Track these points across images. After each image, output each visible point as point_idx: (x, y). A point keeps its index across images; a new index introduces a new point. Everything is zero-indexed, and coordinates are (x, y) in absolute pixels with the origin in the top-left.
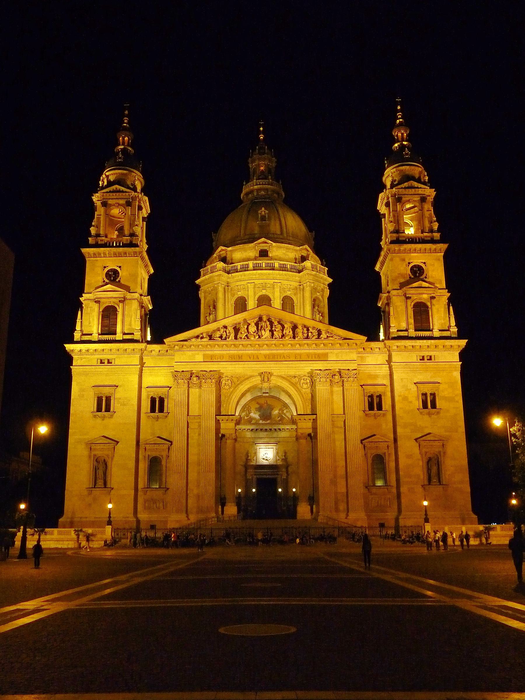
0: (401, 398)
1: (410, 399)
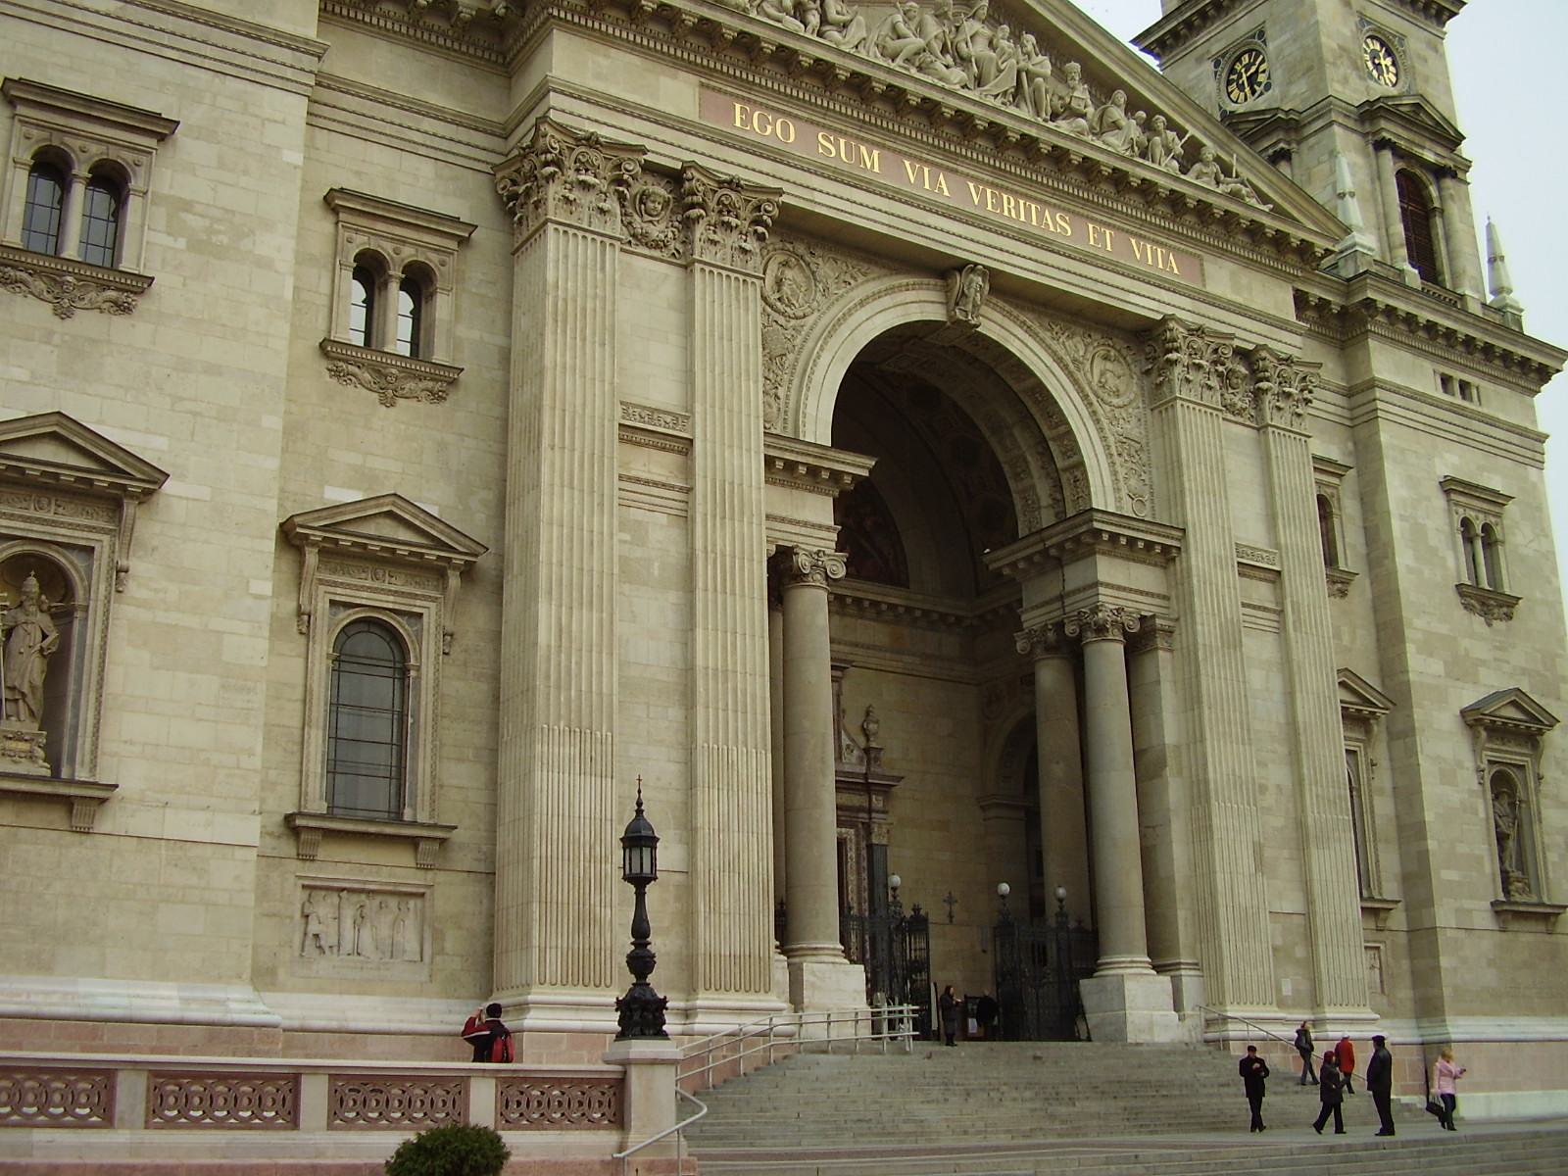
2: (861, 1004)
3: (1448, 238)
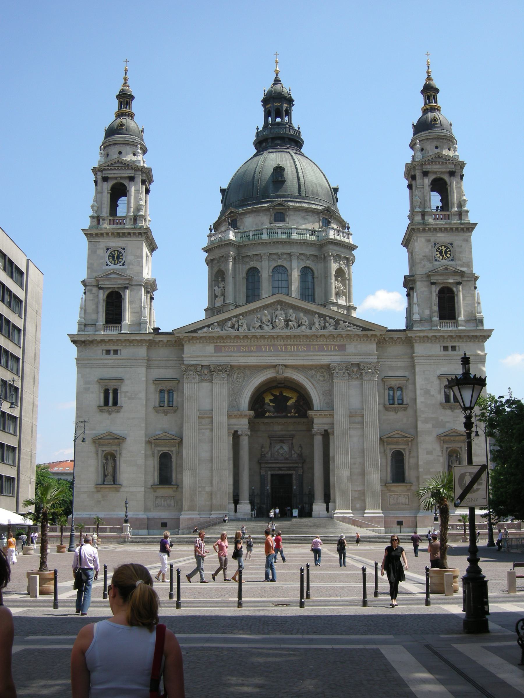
0: (422, 391)
1: (432, 394)
2: (250, 511)
3: (458, 302)
